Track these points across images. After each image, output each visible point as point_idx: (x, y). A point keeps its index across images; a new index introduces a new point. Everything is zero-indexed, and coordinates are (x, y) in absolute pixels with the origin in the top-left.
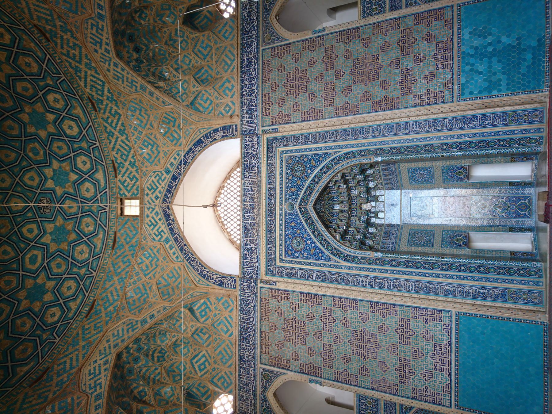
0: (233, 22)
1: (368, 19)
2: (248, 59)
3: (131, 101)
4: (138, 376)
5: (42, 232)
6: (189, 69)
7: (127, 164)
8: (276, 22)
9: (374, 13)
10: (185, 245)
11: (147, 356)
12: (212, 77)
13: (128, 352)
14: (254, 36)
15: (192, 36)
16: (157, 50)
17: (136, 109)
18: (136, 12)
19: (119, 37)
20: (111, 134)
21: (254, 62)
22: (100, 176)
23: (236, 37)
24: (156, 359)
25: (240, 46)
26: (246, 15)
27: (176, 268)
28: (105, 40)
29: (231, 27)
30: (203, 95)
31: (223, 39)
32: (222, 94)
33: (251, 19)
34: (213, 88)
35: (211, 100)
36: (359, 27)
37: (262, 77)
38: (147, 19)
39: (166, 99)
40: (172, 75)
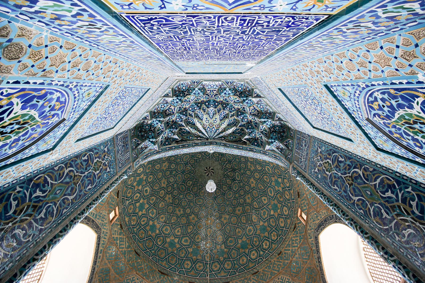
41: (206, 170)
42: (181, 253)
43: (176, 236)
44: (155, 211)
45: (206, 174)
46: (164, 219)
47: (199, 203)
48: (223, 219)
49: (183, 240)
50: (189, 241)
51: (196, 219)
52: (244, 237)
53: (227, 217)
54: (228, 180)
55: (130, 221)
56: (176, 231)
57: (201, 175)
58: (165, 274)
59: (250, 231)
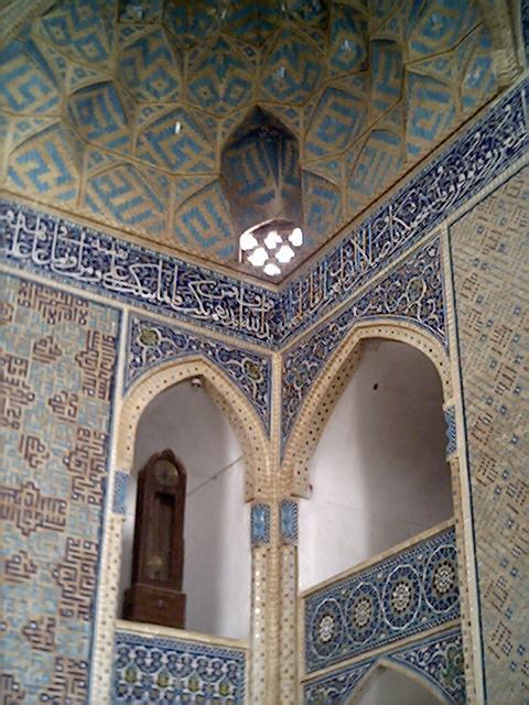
0: (224, 253)
1: (109, 649)
2: (107, 259)
6: (135, 83)
8: (185, 375)
9: (123, 672)
12: (91, 136)
14: (167, 299)
15: (220, 123)
16: (212, 11)
21: (93, 275)
23: (181, 245)
25: (152, 250)
26: (230, 294)
29: (212, 241)
30: (46, 90)
31: (187, 208)
32: (30, 146)
33: (215, 304)
34: (56, 126)
35: (23, 106)
36: (92, 617)
37: (42, 286)
38: (295, 15)
40: (133, 27)
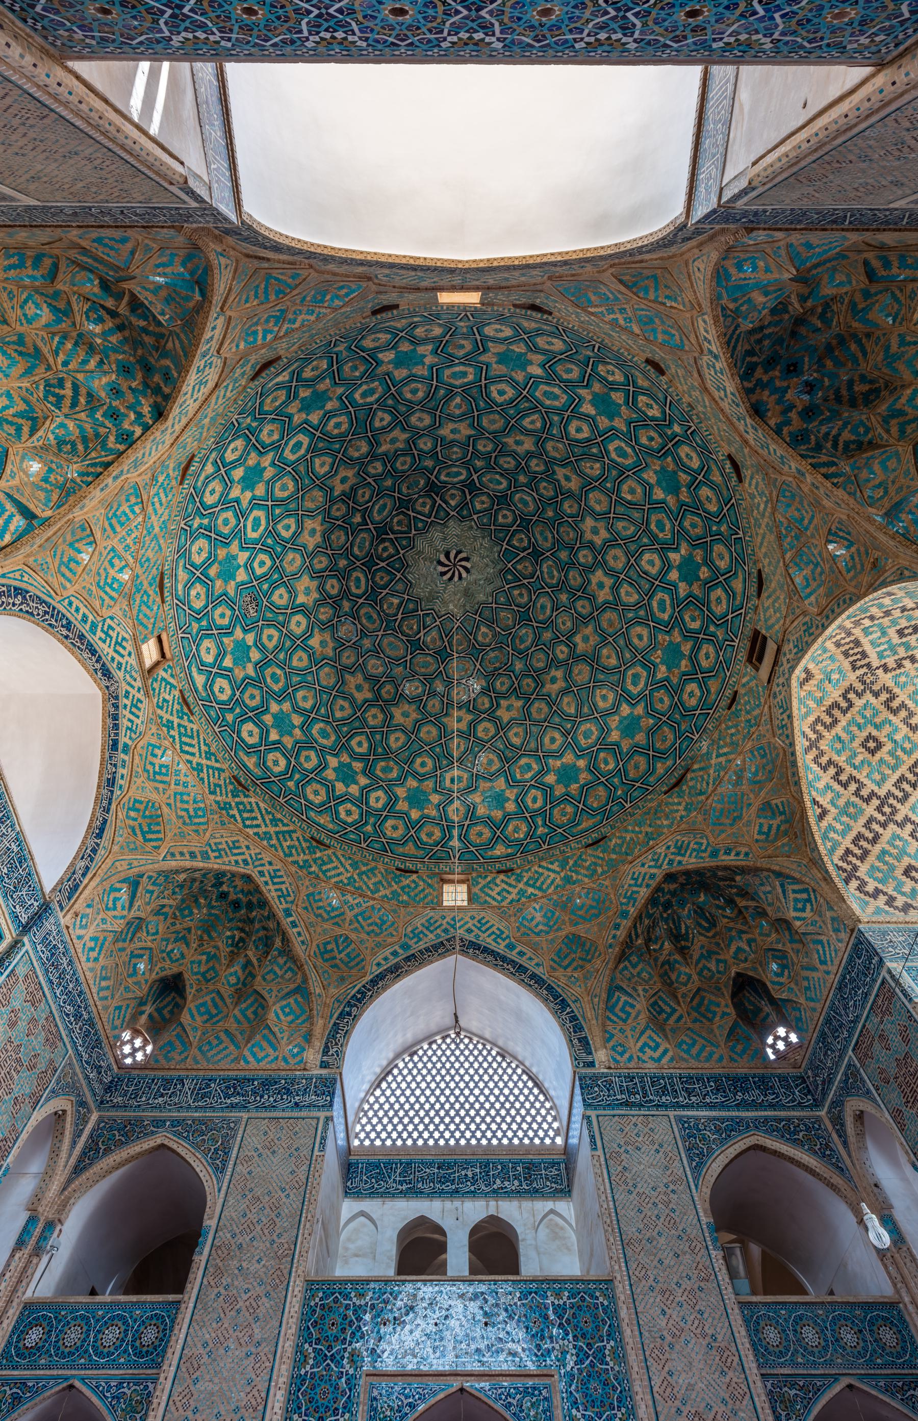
3: (207, 823)
4: (107, 357)
5: (249, 566)
7: (176, 721)
10: (67, 637)
11: (90, 395)
13: (139, 415)
17: (197, 816)
18: (242, 940)
19: (255, 900)
20: (209, 755)
22: (200, 680)
24: (68, 385)
27: (68, 585)
28: (271, 887)
30: (123, 908)
39: (174, 863)
41: (449, 575)
42: (659, 706)
43: (614, 709)
44: (523, 761)
45: (464, 575)
46: (557, 735)
47: (548, 612)
48: (598, 541)
49: (631, 688)
50: (639, 669)
51: (588, 630)
52: (645, 476)
53: (589, 522)
54: (478, 506)
55: (508, 842)
56: (601, 704)
57: (467, 593)
58: (683, 776)
59: (621, 452)
